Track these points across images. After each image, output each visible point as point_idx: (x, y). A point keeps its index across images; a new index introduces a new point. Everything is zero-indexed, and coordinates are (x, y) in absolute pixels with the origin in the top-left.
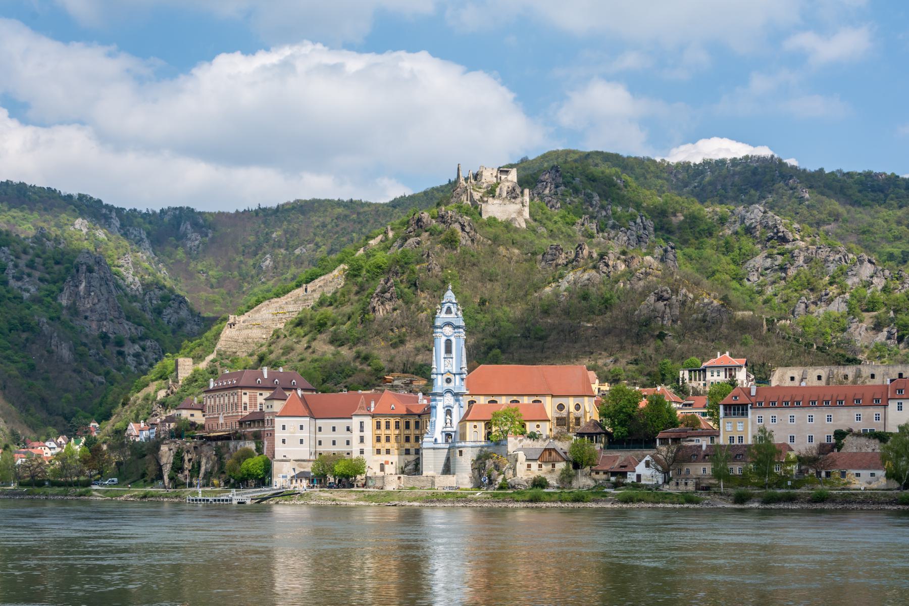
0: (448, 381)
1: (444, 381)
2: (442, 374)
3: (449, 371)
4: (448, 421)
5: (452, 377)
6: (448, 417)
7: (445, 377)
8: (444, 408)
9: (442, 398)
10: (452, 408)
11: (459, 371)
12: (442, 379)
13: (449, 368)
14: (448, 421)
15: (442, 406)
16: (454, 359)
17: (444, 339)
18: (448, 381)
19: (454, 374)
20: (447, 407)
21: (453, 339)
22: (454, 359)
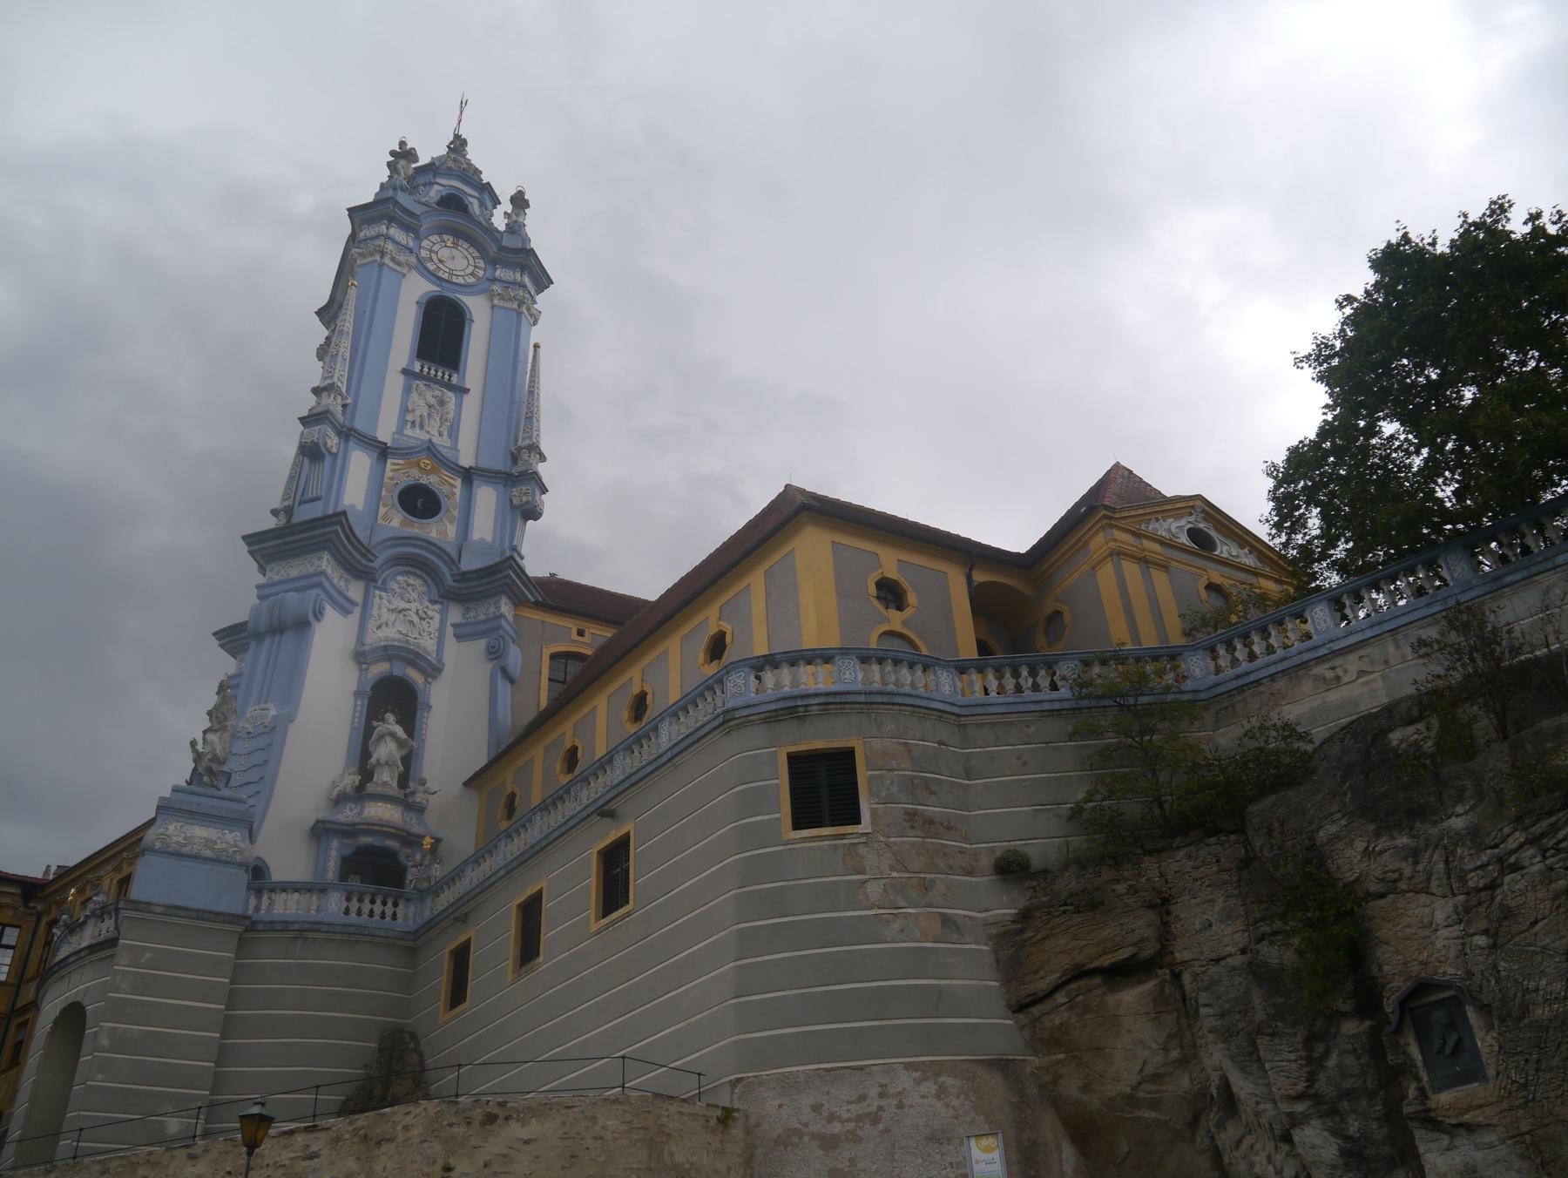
0: (420, 502)
1: (390, 496)
2: (383, 452)
3: (430, 449)
4: (386, 750)
5: (450, 489)
6: (391, 724)
7: (398, 474)
8: (361, 657)
9: (355, 591)
10: (433, 670)
11: (498, 463)
12: (377, 481)
13: (434, 433)
14: (386, 750)
15: (351, 645)
16: (471, 404)
17: (415, 289)
18: (420, 502)
19: (468, 475)
20: (388, 652)
21: (477, 308)
22: (471, 404)
